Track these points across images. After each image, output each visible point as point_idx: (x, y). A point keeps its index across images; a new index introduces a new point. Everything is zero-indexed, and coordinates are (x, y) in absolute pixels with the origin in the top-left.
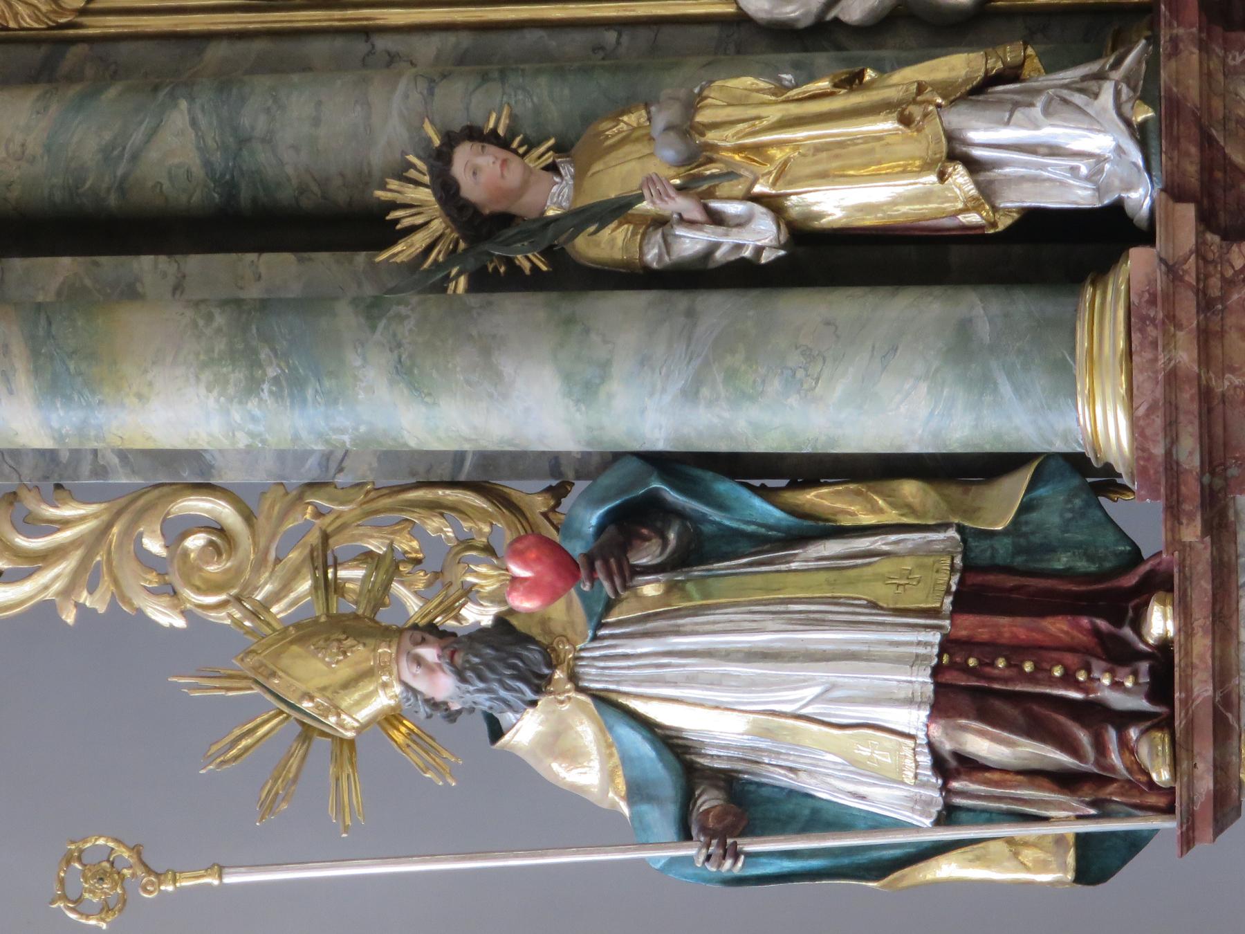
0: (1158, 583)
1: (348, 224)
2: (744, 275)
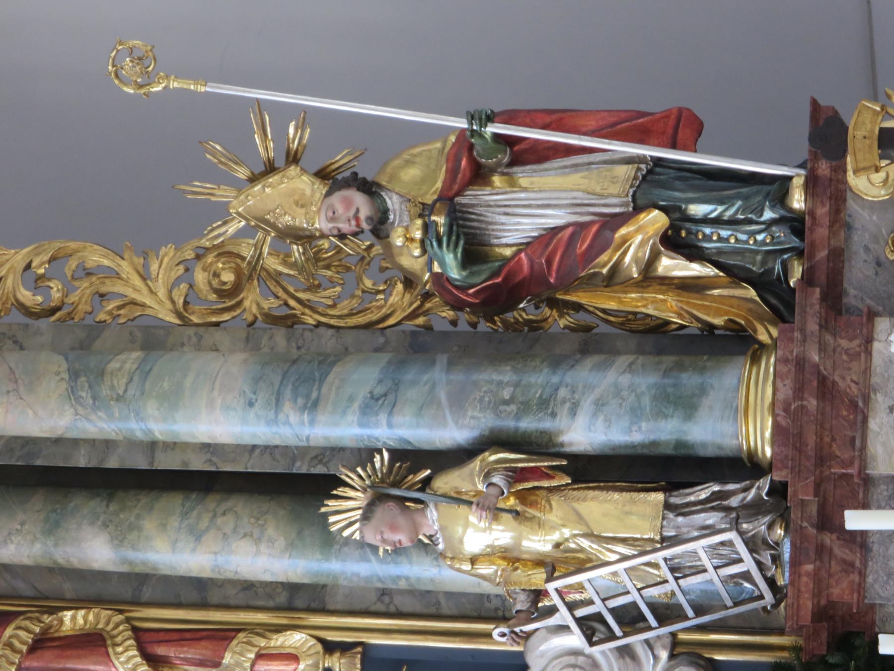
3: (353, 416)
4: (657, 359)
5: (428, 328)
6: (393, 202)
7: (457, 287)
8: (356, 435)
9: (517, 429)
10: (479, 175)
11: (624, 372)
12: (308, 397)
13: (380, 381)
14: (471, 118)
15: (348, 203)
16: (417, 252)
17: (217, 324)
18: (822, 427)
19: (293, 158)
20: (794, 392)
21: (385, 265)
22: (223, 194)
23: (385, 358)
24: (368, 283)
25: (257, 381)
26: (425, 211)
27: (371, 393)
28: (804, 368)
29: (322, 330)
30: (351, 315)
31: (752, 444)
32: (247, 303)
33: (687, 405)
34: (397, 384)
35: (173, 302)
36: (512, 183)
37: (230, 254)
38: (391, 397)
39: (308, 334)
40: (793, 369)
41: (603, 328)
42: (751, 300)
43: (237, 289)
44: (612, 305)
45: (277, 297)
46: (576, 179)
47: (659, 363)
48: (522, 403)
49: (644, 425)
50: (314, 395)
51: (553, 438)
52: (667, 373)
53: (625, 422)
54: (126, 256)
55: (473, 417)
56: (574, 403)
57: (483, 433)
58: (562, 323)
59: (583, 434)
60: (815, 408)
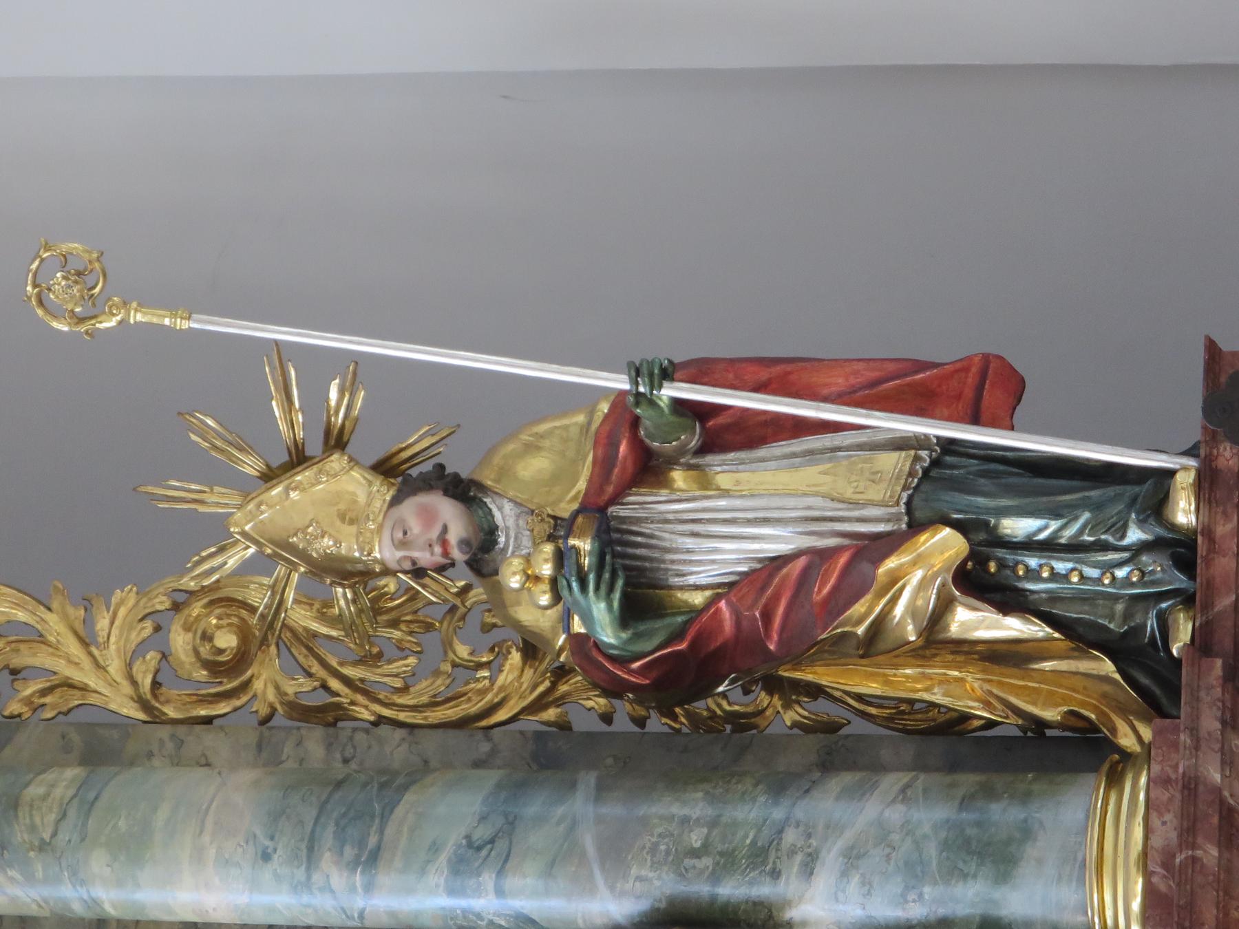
3: (437, 876)
4: (949, 779)
5: (563, 726)
6: (504, 514)
7: (612, 659)
8: (443, 909)
9: (713, 899)
10: (649, 469)
11: (893, 801)
12: (361, 844)
13: (483, 818)
14: (636, 372)
15: (428, 517)
16: (545, 600)
17: (208, 721)
18: (1226, 893)
19: (336, 441)
20: (1180, 836)
21: (490, 619)
22: (218, 500)
23: (492, 777)
24: (463, 651)
25: (275, 817)
26: (559, 529)
27: (468, 837)
28: (1196, 796)
29: (384, 730)
30: (433, 704)
31: (1110, 922)
32: (258, 685)
33: (1001, 857)
34: (512, 823)
35: (134, 683)
36: (705, 483)
37: (230, 601)
38: (501, 845)
39: (360, 737)
40: (1178, 796)
41: (859, 727)
42: (1106, 679)
43: (242, 659)
44: (873, 688)
45: (310, 675)
46: (812, 475)
47: (952, 785)
48: (721, 854)
49: (927, 890)
50: (372, 841)
51: (775, 913)
52: (966, 802)
53: (895, 886)
54: (55, 605)
55: (639, 878)
56: (810, 855)
57: (657, 905)
58: (789, 717)
60: (1216, 861)
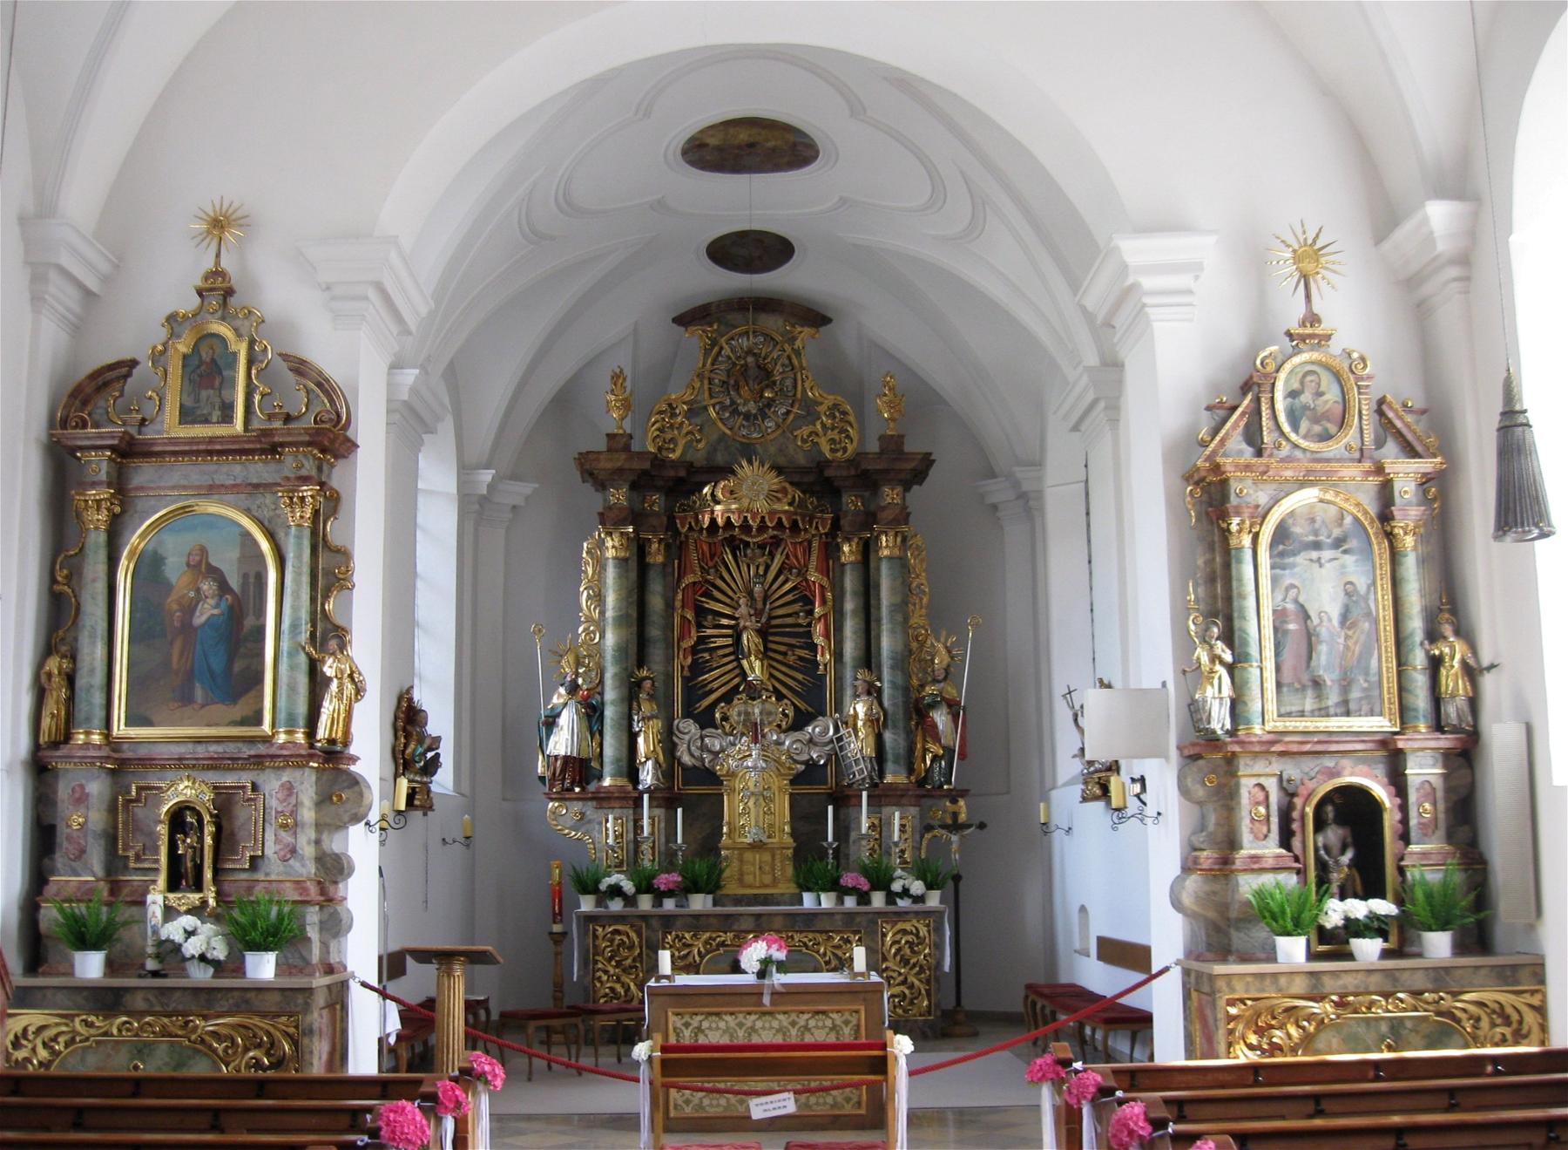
0: (583, 789)
1: (641, 661)
2: (630, 726)
26: (940, 694)
33: (896, 762)
59: (888, 736)
